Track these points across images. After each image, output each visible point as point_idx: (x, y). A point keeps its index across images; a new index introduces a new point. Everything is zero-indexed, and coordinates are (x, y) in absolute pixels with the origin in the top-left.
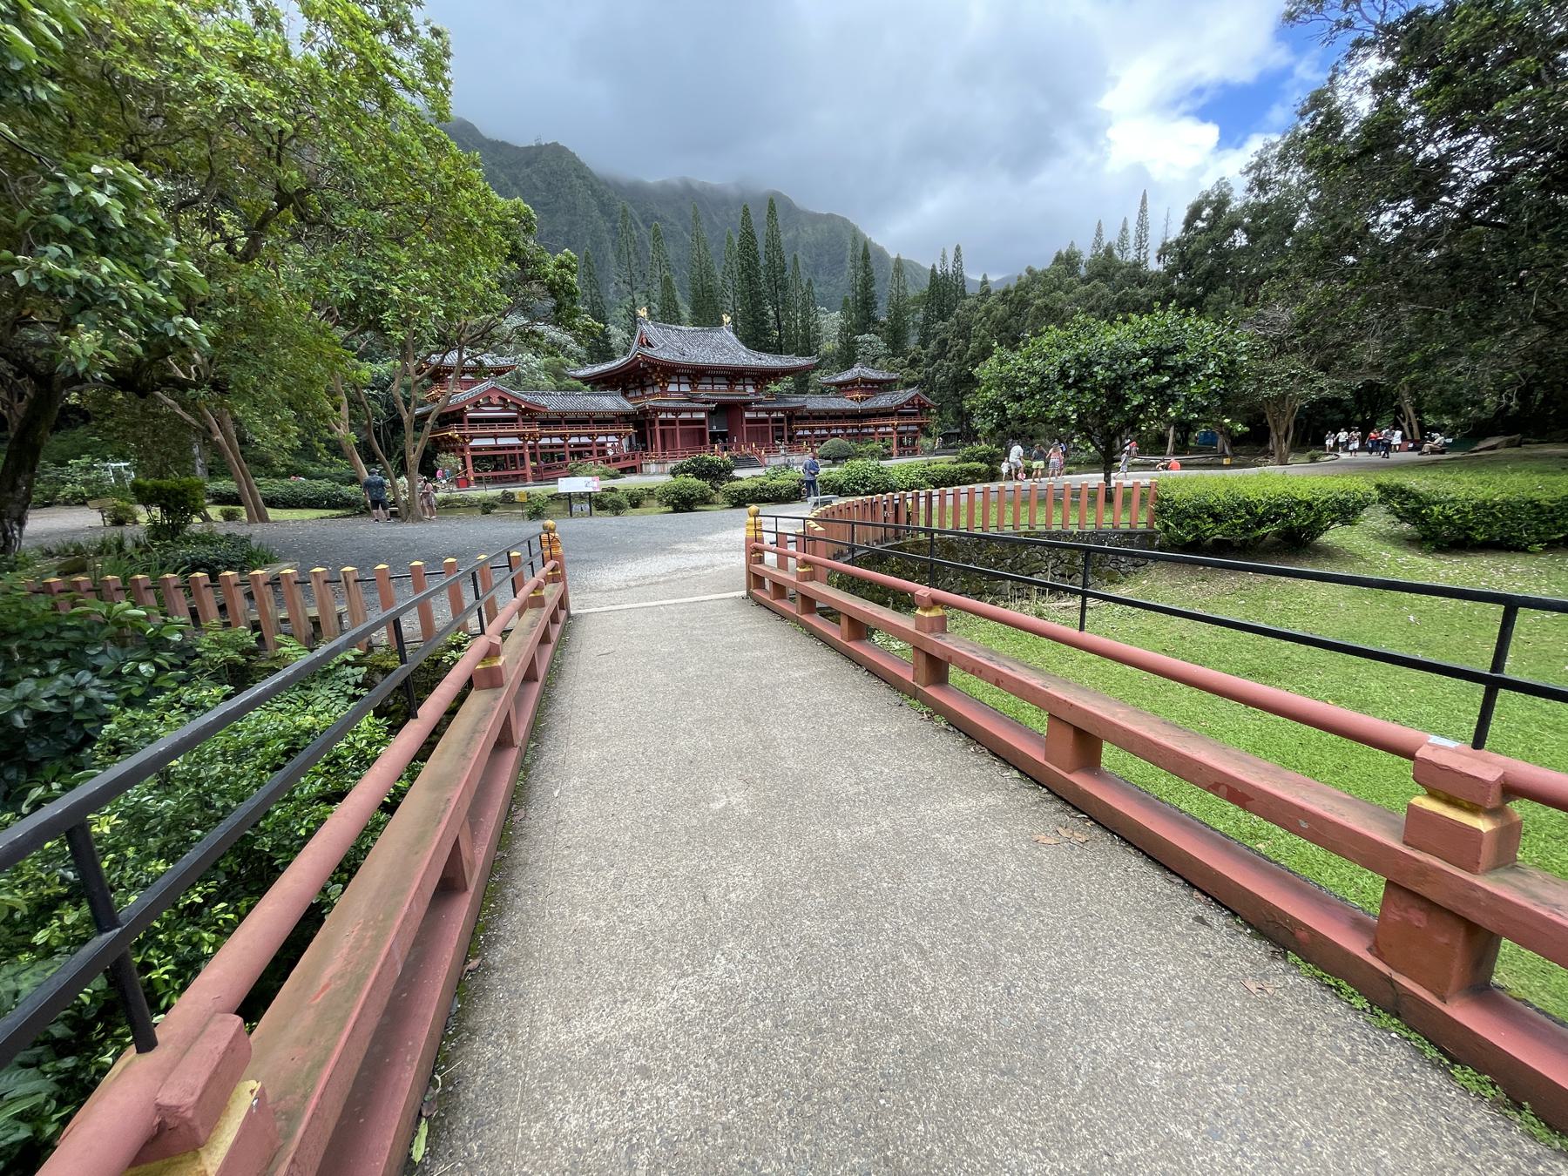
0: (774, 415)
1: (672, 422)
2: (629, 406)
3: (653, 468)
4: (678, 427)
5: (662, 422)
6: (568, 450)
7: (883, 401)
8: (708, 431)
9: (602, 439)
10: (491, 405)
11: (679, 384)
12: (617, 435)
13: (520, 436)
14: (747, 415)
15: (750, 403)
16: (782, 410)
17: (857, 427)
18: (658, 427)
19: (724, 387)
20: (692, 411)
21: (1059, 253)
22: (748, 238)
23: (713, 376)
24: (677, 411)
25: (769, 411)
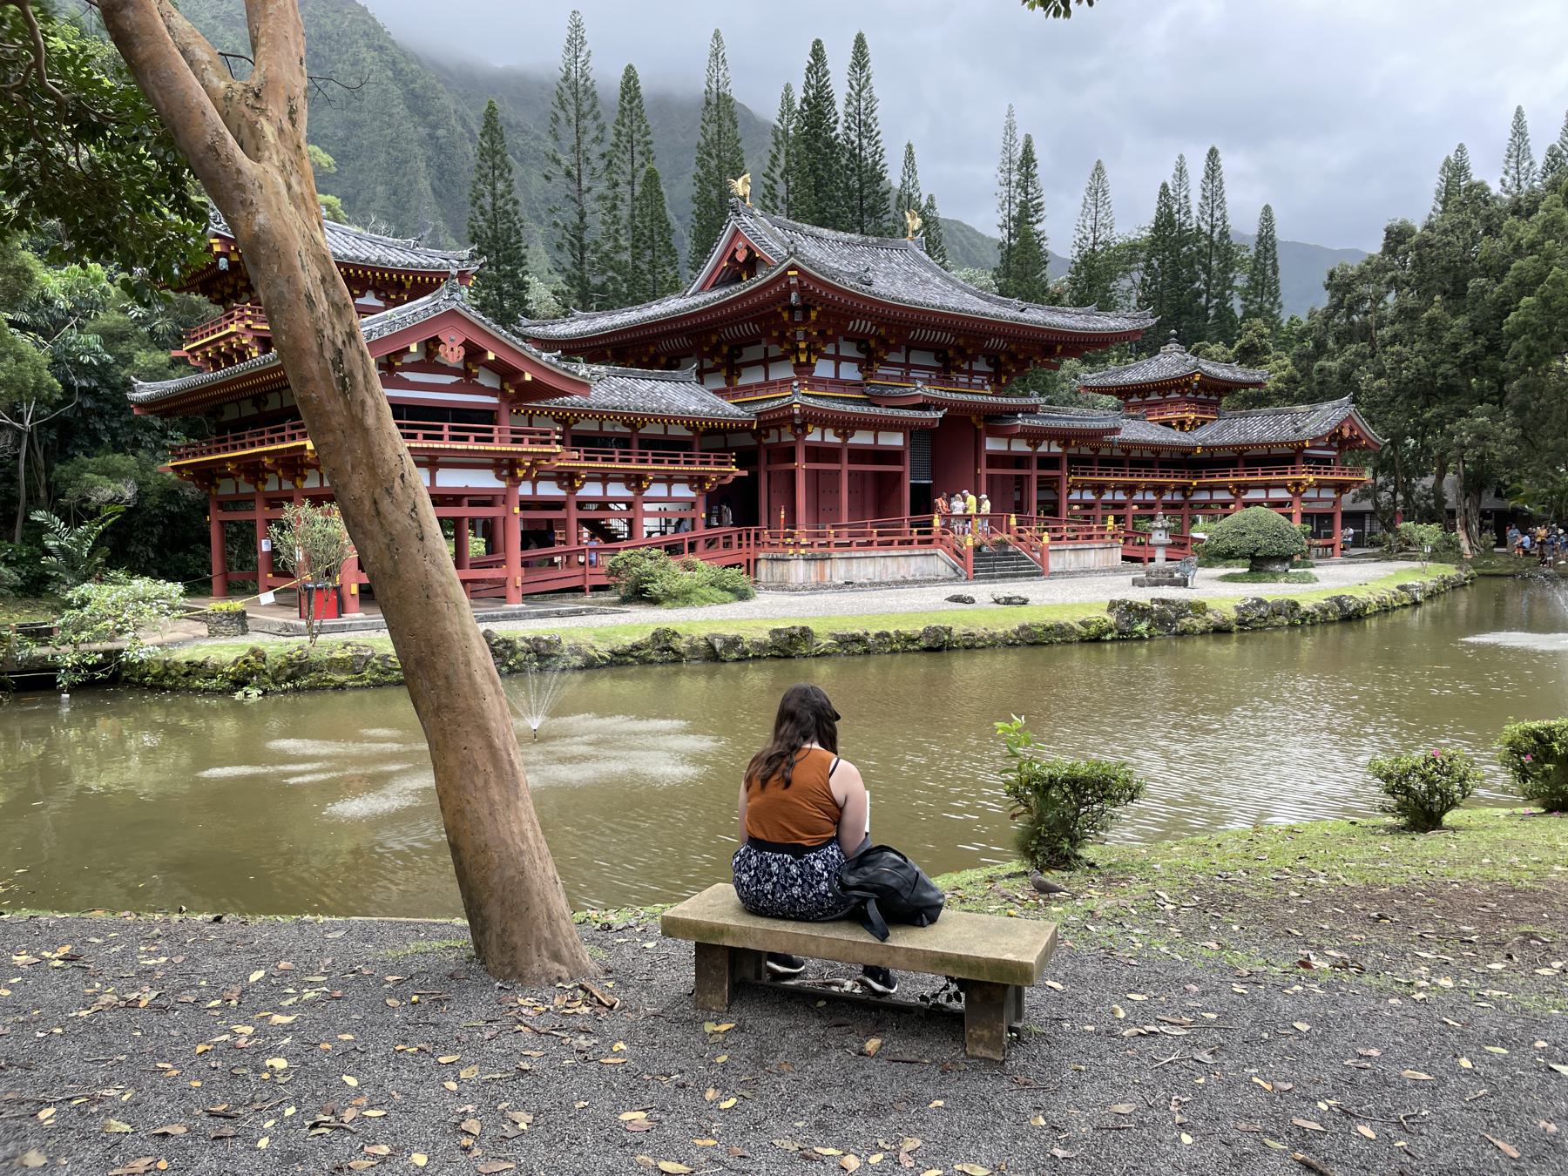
0: (1043, 449)
2: (727, 408)
3: (799, 571)
4: (845, 467)
6: (574, 515)
7: (1258, 428)
8: (908, 482)
9: (658, 490)
11: (838, 359)
12: (696, 481)
13: (506, 466)
14: (992, 445)
15: (1012, 412)
16: (1064, 437)
17: (1184, 489)
18: (801, 465)
20: (877, 426)
21: (1448, 159)
22: (817, 105)
23: (912, 346)
24: (845, 425)
25: (1034, 437)
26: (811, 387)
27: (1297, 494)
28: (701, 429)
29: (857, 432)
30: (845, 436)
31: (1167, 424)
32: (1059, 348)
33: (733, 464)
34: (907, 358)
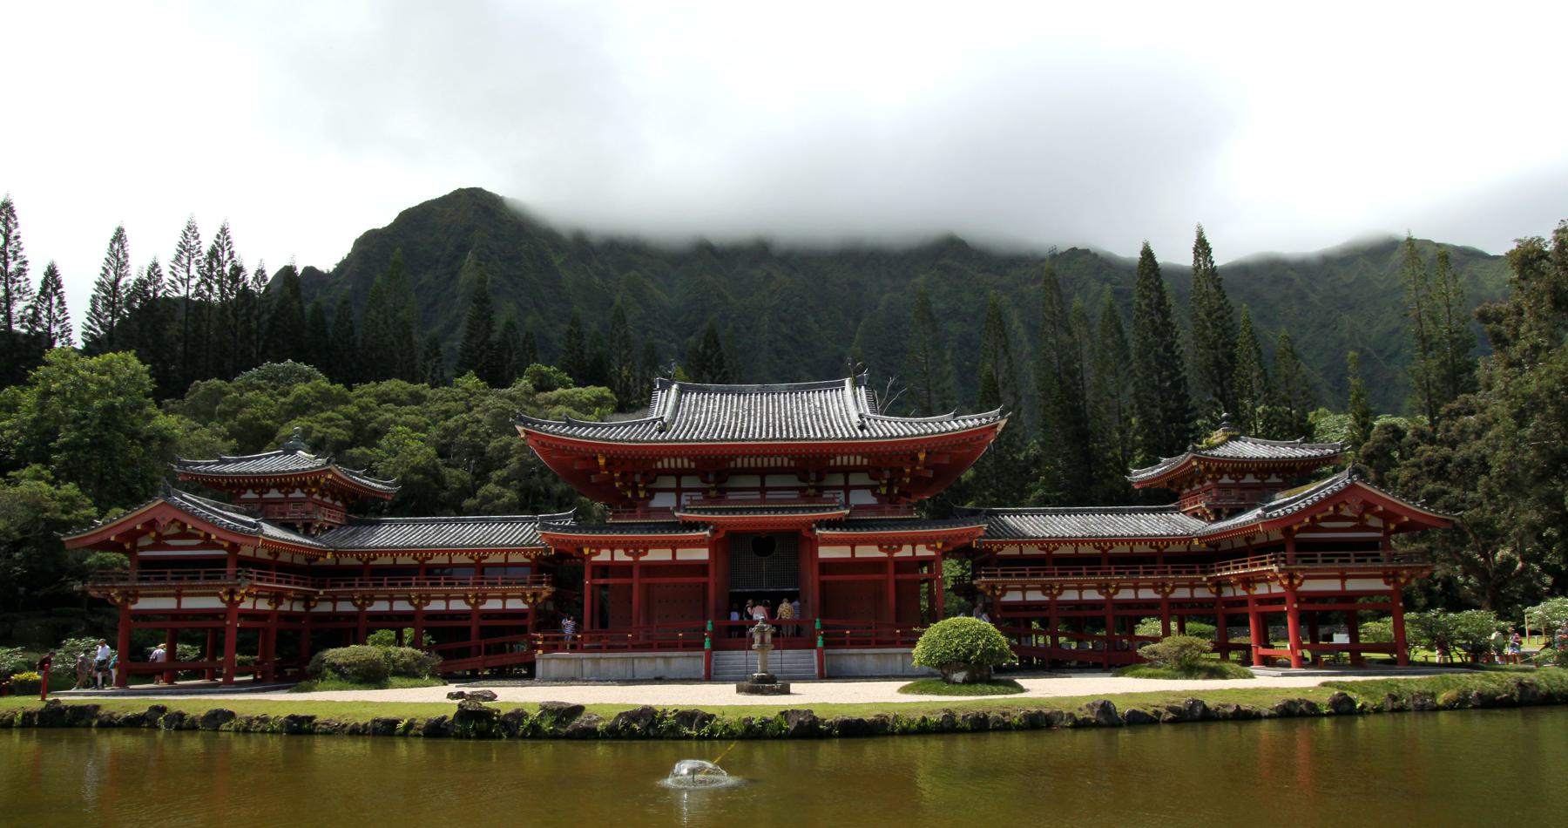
0: (906, 551)
1: (625, 569)
5: (605, 569)
10: (184, 534)
11: (678, 491)
19: (795, 495)
20: (674, 546)
26: (614, 518)
27: (1282, 585)
28: (533, 556)
29: (650, 551)
30: (636, 555)
31: (1195, 515)
32: (922, 457)
33: (548, 583)
34: (763, 482)
